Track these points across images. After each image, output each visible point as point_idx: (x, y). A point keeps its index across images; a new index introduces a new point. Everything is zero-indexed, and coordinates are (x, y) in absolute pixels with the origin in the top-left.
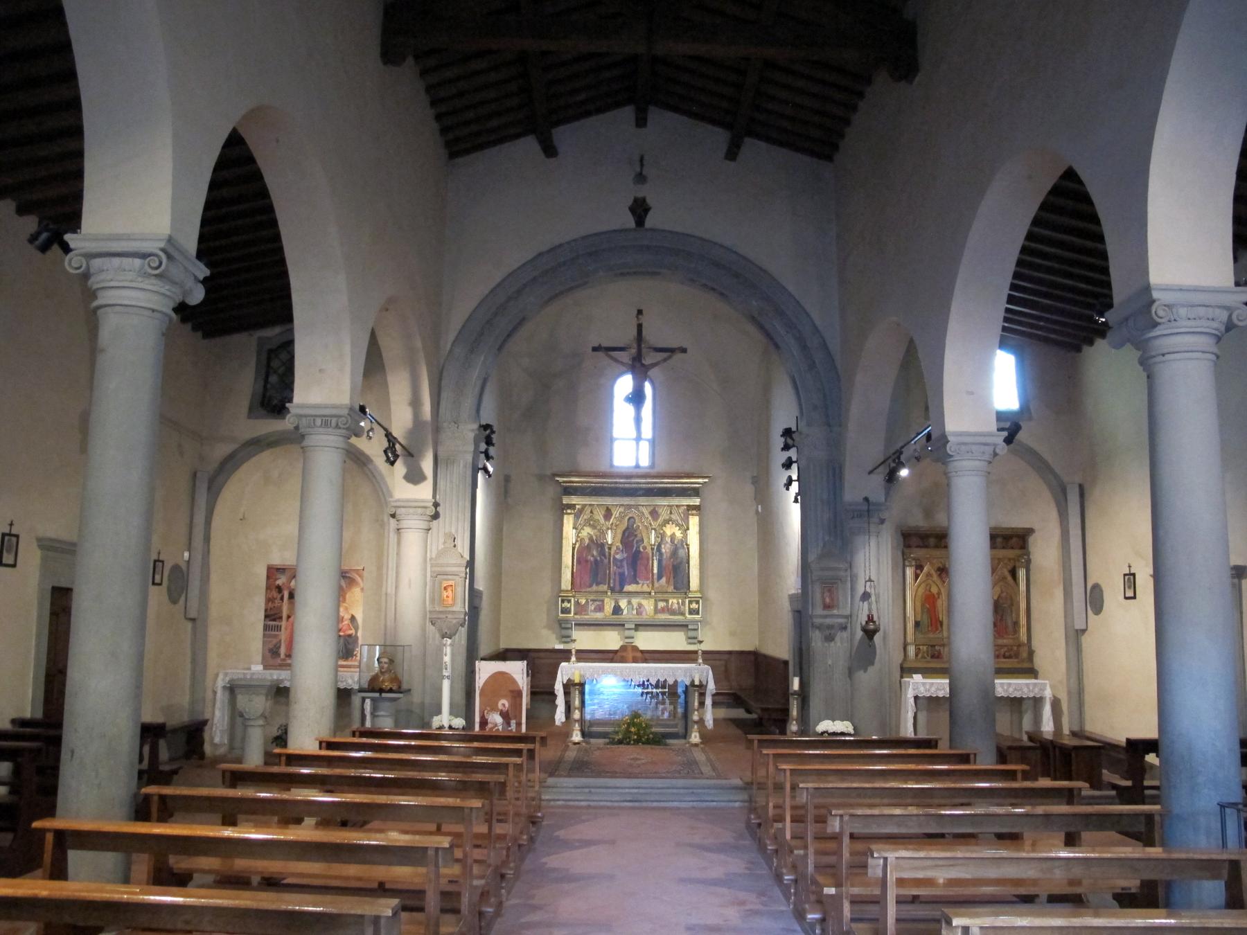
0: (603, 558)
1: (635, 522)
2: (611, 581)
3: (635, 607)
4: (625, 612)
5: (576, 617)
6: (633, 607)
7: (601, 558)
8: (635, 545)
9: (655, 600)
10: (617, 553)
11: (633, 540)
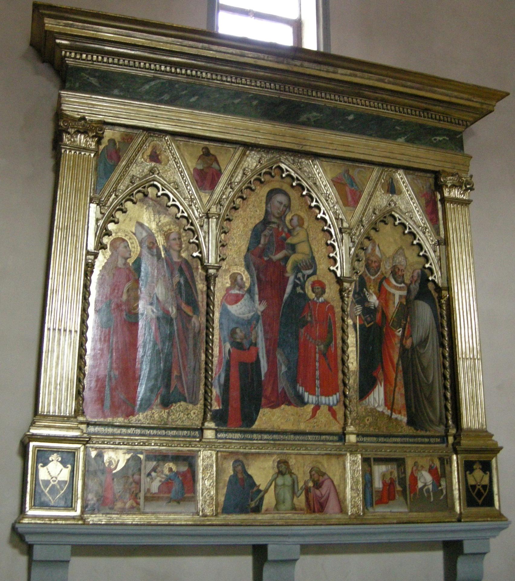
0: (188, 310)
1: (288, 207)
2: (216, 391)
3: (301, 484)
4: (269, 499)
5: (92, 519)
6: (294, 483)
7: (179, 308)
8: (291, 279)
9: (366, 460)
10: (237, 299)
11: (286, 259)
